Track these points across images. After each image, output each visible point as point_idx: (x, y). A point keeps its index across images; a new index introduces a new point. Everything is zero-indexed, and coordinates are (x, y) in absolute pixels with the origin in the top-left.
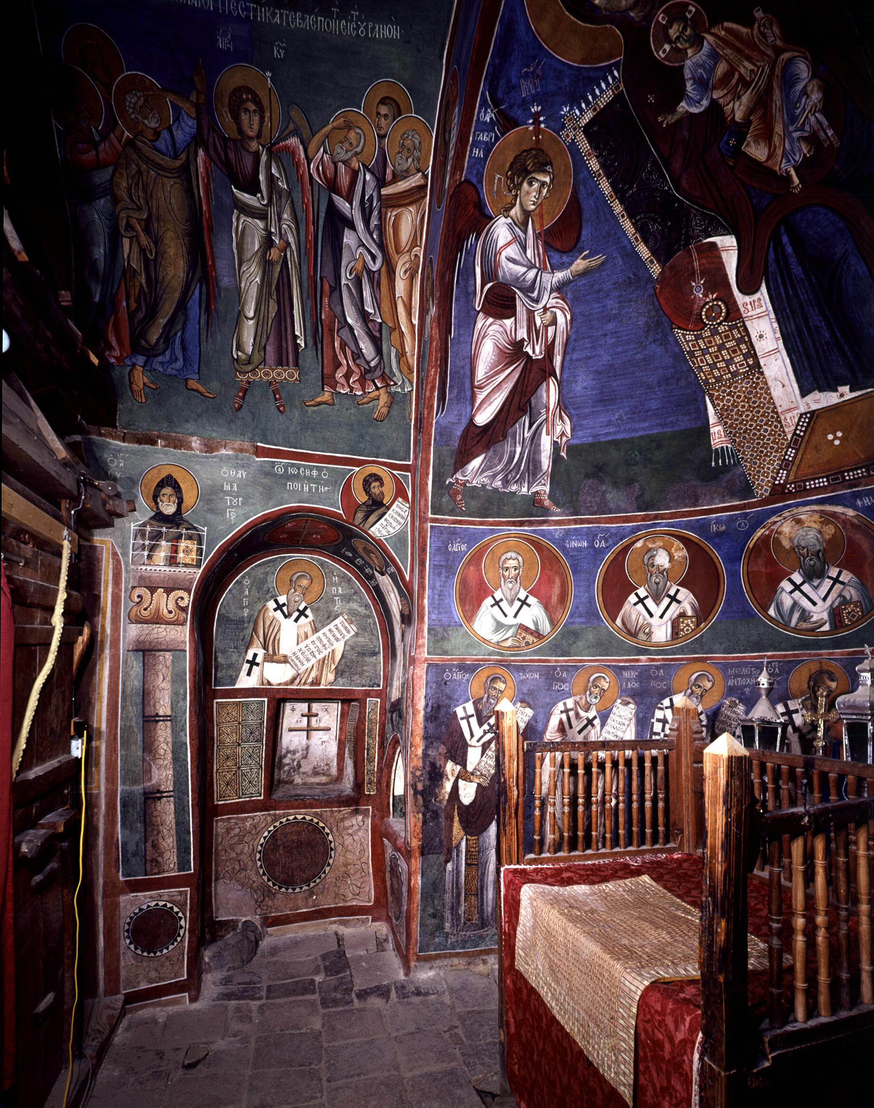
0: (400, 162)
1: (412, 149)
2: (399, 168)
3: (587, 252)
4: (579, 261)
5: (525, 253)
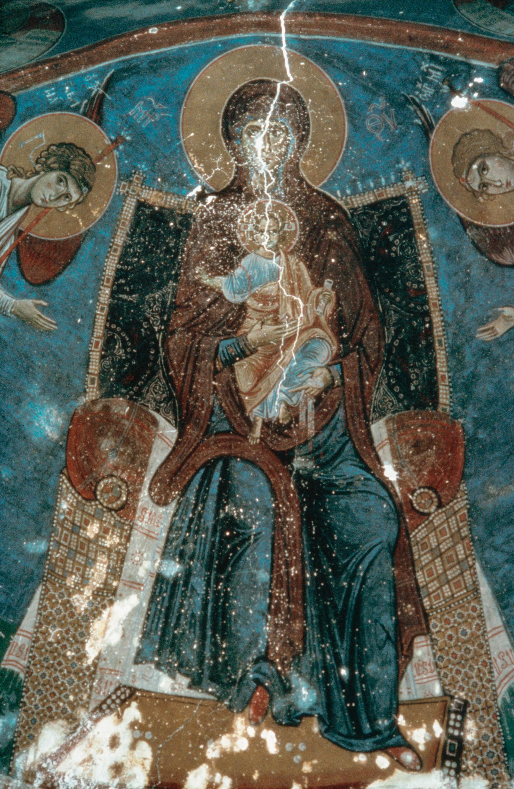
3: (45, 304)
4: (30, 302)
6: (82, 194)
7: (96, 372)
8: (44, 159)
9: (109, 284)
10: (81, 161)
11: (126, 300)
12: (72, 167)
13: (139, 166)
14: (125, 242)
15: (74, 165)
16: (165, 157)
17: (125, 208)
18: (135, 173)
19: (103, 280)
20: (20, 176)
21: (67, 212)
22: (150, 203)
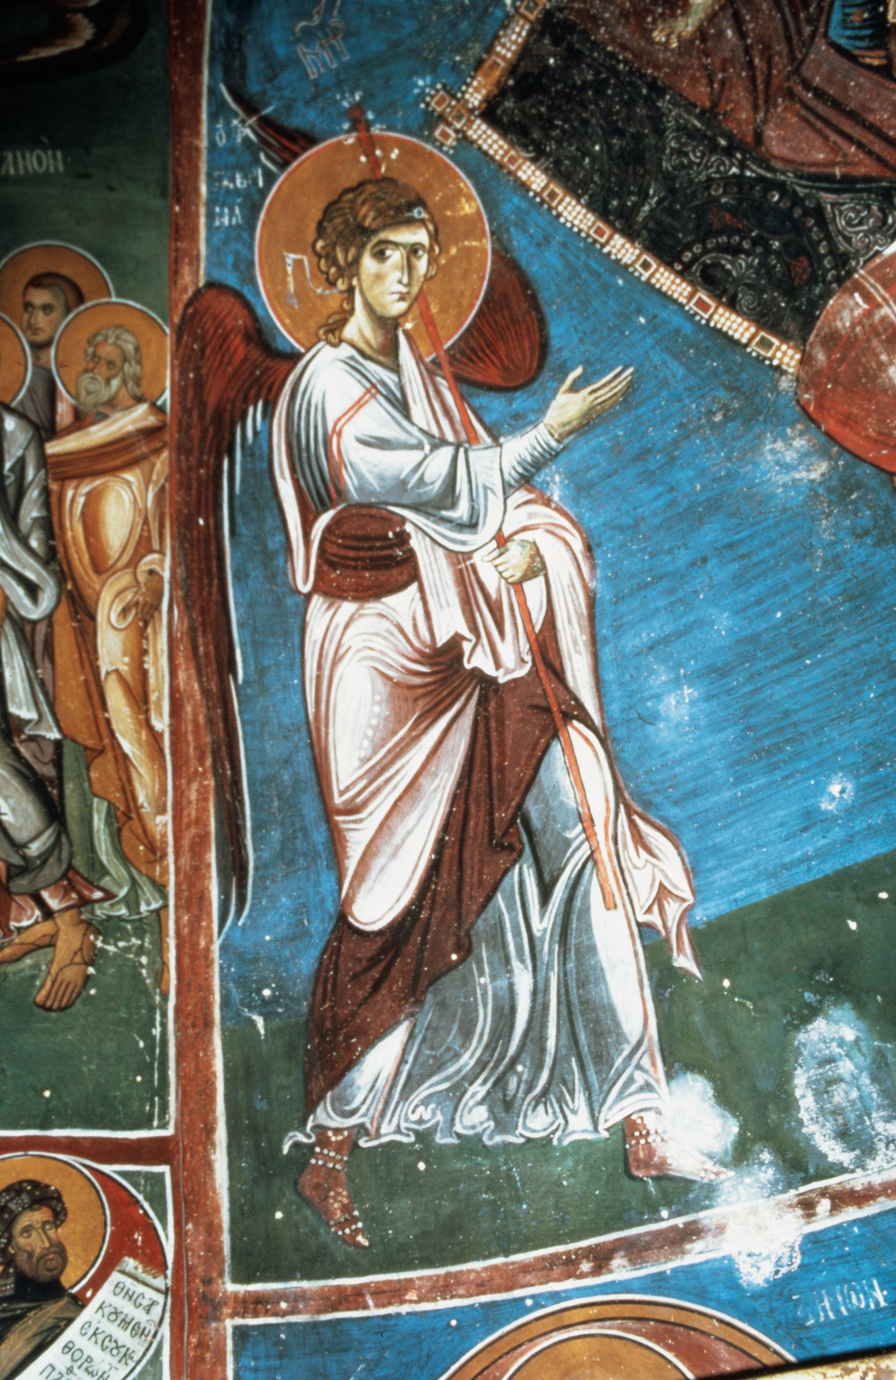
0: (92, 387)
1: (118, 362)
2: (90, 400)
6: (422, 222)
7: (753, 330)
9: (608, 232)
10: (364, 202)
11: (652, 210)
12: (367, 224)
13: (416, 91)
14: (546, 171)
15: (365, 217)
18: (428, 104)
19: (595, 241)
21: (443, 261)
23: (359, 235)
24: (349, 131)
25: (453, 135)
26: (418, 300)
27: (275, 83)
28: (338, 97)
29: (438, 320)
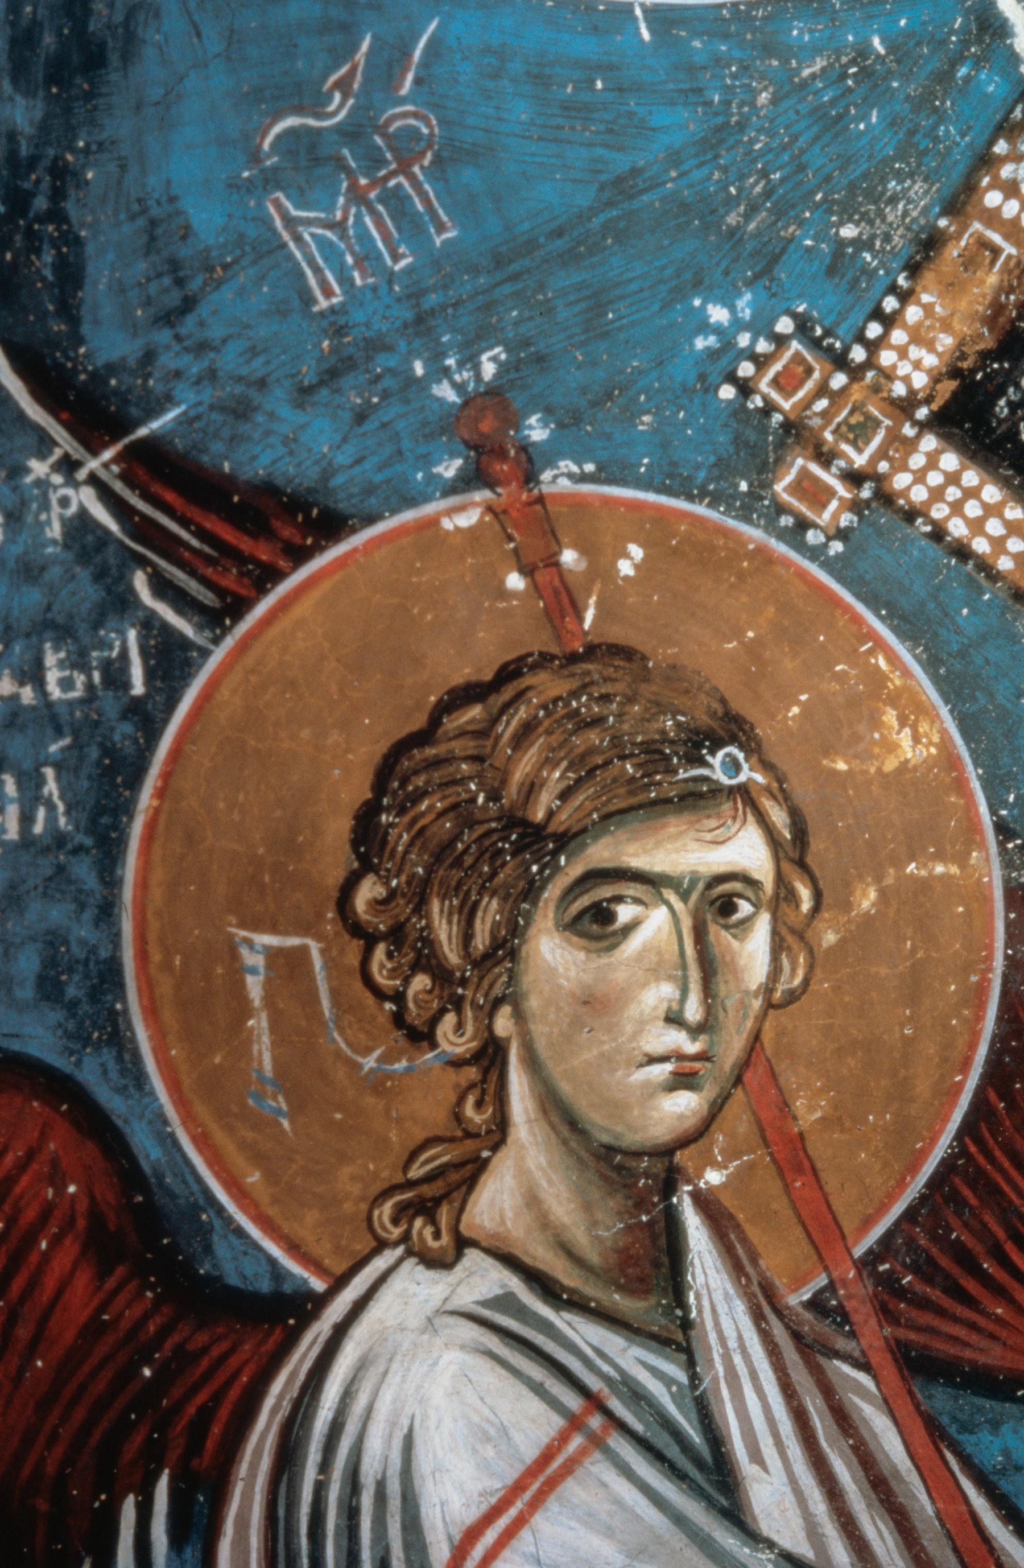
5: (735, 1514)
8: (421, 982)
15: (532, 788)
16: (715, 140)
17: (957, 528)
18: (745, 388)
20: (470, 1172)
22: (988, 341)
23: (514, 852)
24: (464, 483)
25: (842, 491)
26: (745, 1080)
27: (189, 324)
28: (419, 369)
29: (819, 1149)
